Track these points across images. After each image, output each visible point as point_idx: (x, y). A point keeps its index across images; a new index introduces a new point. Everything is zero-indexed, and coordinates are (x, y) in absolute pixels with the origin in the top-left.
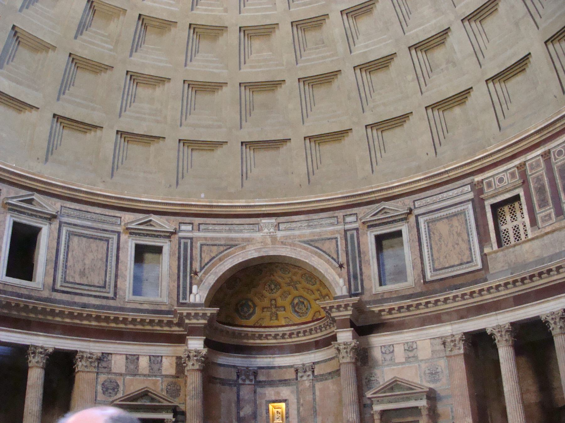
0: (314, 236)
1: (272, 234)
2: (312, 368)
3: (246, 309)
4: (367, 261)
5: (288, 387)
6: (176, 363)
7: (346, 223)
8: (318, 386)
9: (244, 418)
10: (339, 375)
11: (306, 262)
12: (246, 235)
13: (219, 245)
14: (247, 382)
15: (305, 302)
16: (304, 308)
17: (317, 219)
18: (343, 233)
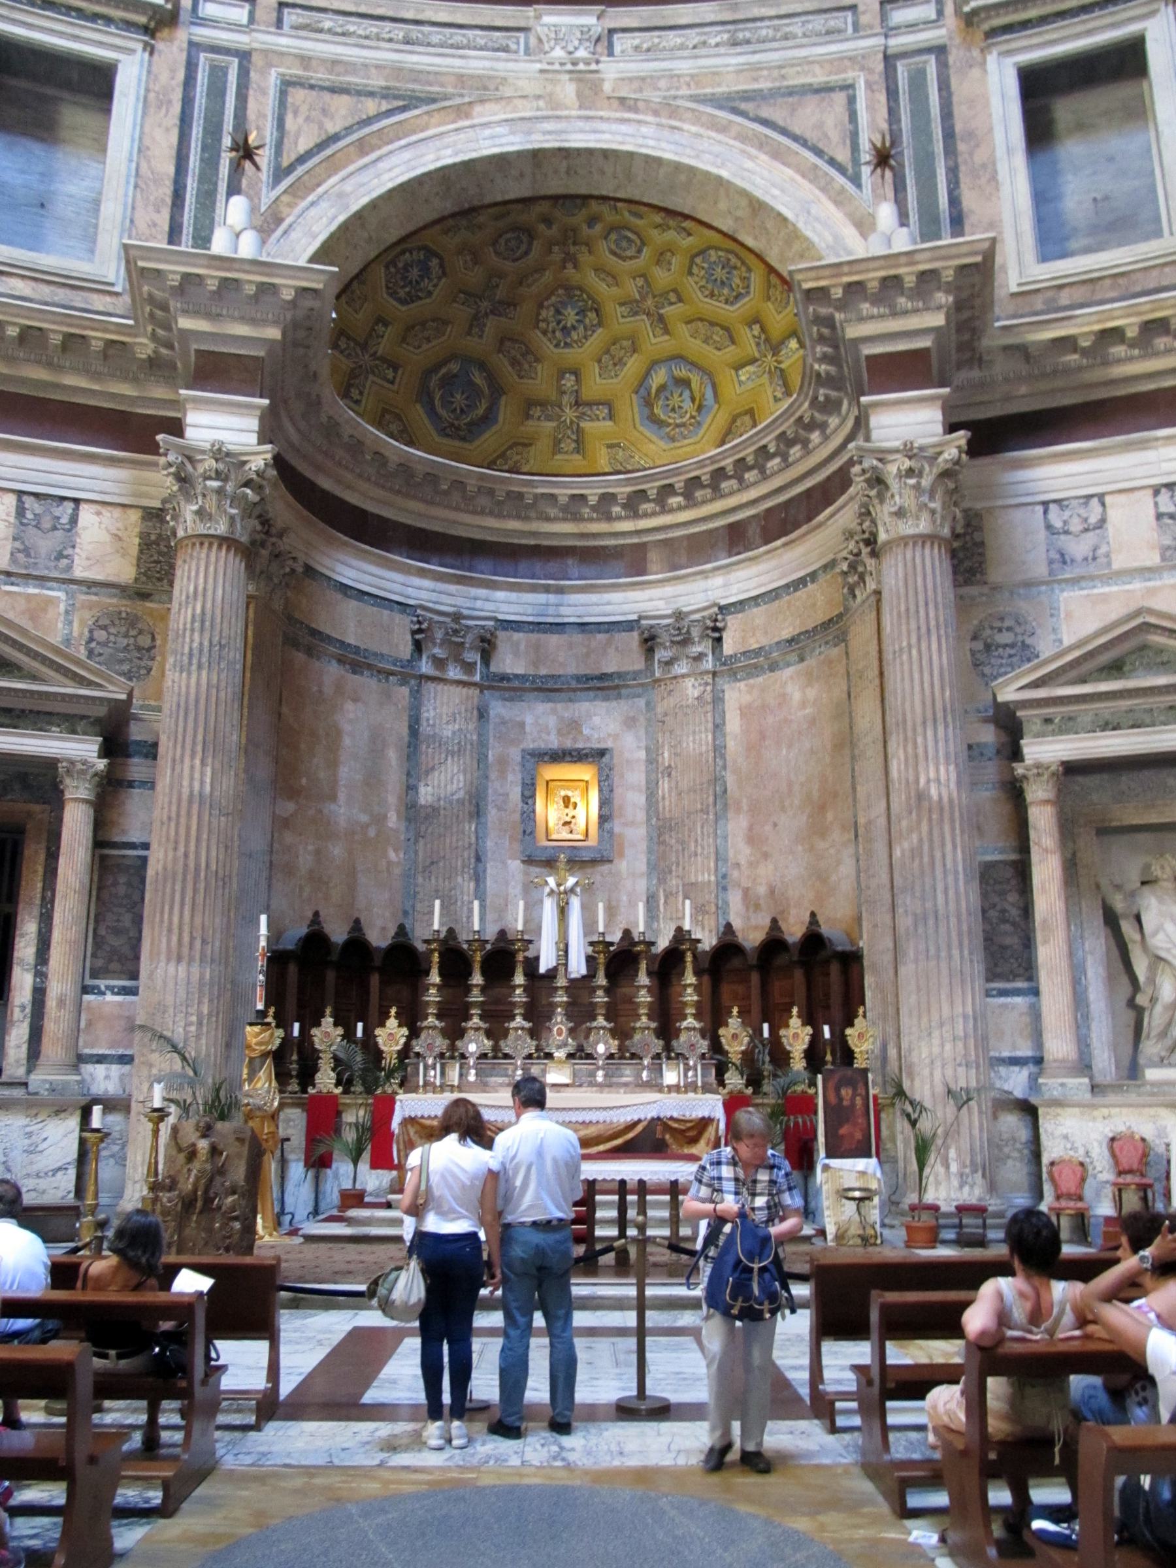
0: (755, 80)
1: (581, 67)
2: (715, 629)
3: (459, 398)
4: (984, 166)
5: (614, 704)
6: (143, 536)
7: (892, 29)
8: (736, 695)
9: (434, 811)
10: (842, 638)
11: (719, 180)
12: (477, 63)
13: (359, 93)
14: (454, 672)
15: (695, 379)
16: (687, 405)
17: (771, 18)
18: (880, 67)
